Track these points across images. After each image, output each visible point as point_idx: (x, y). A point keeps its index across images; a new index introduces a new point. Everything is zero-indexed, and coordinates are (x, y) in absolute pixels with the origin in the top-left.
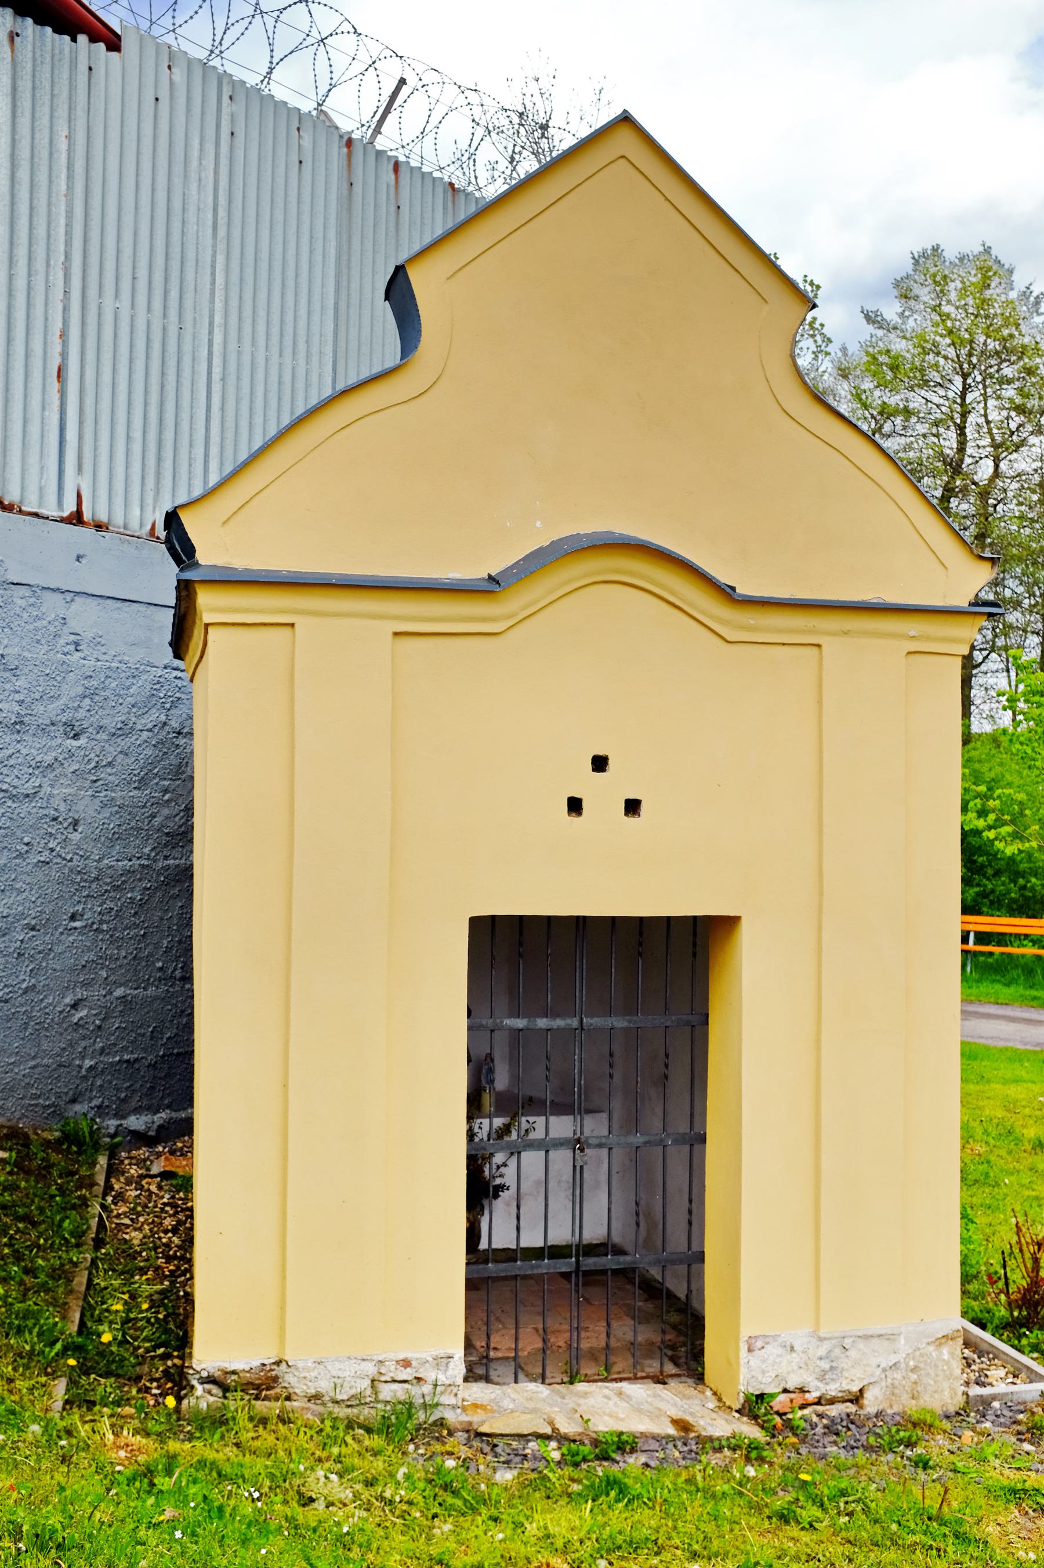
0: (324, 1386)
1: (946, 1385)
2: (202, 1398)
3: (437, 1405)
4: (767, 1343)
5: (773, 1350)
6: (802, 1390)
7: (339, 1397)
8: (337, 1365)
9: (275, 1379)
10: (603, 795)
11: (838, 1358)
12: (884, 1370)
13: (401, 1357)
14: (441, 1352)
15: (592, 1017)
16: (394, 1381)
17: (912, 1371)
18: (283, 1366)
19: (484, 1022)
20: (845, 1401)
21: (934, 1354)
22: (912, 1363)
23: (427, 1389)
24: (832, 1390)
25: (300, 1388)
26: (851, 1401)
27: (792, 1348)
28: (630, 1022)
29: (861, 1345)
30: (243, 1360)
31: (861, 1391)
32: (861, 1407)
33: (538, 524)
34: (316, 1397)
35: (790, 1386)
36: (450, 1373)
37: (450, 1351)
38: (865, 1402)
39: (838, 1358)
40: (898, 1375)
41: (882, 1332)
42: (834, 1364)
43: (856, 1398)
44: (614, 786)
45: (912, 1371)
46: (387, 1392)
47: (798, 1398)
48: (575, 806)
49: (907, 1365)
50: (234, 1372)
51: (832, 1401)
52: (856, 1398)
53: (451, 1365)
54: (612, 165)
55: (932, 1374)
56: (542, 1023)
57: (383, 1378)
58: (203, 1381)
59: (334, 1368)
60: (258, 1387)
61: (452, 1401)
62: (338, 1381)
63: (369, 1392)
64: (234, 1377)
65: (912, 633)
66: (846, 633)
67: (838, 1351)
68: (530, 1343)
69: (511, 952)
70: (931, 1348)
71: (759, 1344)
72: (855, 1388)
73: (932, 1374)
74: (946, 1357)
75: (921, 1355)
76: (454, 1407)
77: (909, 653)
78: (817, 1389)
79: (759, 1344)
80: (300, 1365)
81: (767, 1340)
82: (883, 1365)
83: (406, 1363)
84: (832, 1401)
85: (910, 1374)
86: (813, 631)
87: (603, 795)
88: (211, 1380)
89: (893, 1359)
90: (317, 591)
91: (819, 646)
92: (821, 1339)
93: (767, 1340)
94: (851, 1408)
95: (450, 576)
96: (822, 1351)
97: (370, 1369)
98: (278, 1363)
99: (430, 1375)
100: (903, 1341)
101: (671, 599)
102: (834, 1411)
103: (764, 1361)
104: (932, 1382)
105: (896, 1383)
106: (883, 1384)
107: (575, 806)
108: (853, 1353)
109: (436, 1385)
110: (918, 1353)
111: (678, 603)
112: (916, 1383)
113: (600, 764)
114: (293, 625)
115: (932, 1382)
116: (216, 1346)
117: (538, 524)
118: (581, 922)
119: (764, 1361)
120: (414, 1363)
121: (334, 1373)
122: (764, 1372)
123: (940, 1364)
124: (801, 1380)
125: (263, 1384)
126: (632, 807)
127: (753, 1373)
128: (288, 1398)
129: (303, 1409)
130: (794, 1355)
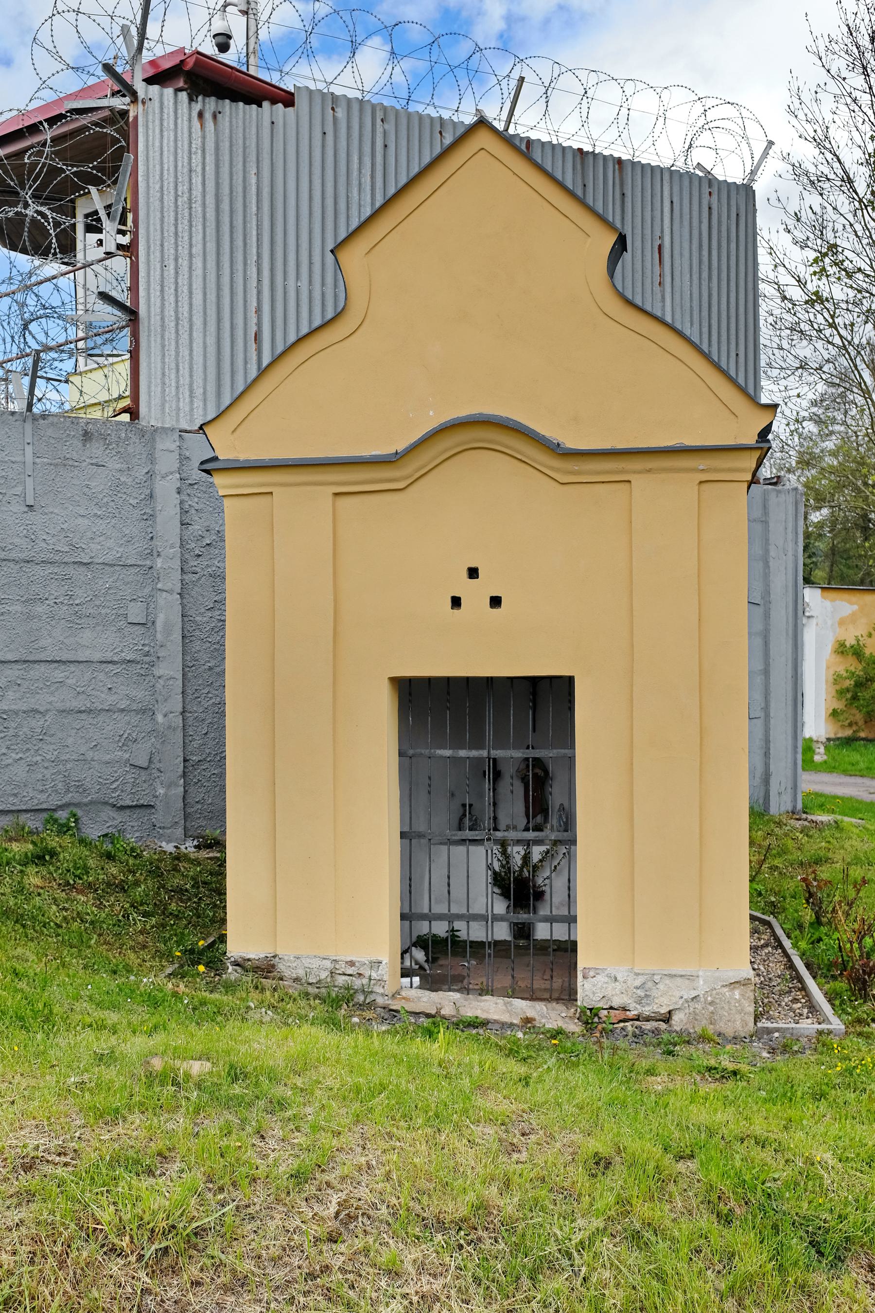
0: (301, 973)
1: (738, 1017)
2: (232, 973)
3: (372, 992)
4: (598, 974)
5: (601, 979)
6: (625, 1009)
7: (311, 981)
8: (308, 960)
9: (273, 966)
10: (475, 595)
11: (650, 989)
12: (687, 1001)
13: (349, 959)
14: (374, 959)
15: (497, 749)
16: (345, 974)
17: (710, 1004)
18: (277, 959)
19: (423, 751)
20: (657, 1020)
21: (727, 994)
22: (709, 998)
23: (365, 981)
24: (647, 1011)
25: (287, 973)
26: (664, 1021)
27: (616, 979)
28: (523, 753)
29: (667, 981)
30: (255, 952)
31: (670, 1012)
32: (670, 1026)
33: (431, 413)
34: (297, 980)
35: (615, 1004)
36: (380, 972)
37: (380, 959)
38: (673, 1022)
39: (650, 989)
40: (699, 1006)
41: (683, 973)
42: (648, 993)
43: (667, 1018)
44: (483, 588)
45: (710, 1004)
46: (341, 980)
47: (620, 1015)
48: (456, 602)
49: (706, 999)
50: (249, 960)
51: (648, 1019)
52: (667, 1018)
53: (381, 968)
54: (476, 156)
55: (727, 1008)
56: (463, 753)
57: (338, 972)
58: (236, 964)
59: (306, 962)
60: (263, 970)
61: (381, 991)
62: (308, 970)
63: (329, 980)
64: (250, 963)
65: (701, 467)
66: (649, 471)
67: (650, 984)
68: (507, 981)
69: (426, 703)
70: (725, 990)
71: (592, 973)
72: (664, 1010)
73: (727, 1008)
74: (737, 997)
75: (717, 994)
76: (382, 995)
77: (701, 482)
78: (636, 1009)
79: (592, 973)
80: (286, 958)
81: (597, 971)
82: (685, 997)
83: (352, 964)
84: (648, 1019)
85: (708, 1006)
86: (623, 471)
87: (475, 595)
88: (236, 964)
89: (693, 994)
90: (310, 469)
91: (629, 481)
92: (637, 974)
93: (597, 971)
94: (663, 1026)
95: (374, 453)
96: (638, 983)
97: (328, 964)
98: (274, 957)
99: (367, 973)
100: (701, 982)
101: (519, 457)
102: (648, 1026)
103: (594, 986)
104: (726, 1014)
105: (697, 1011)
106: (687, 1011)
107: (456, 602)
108: (661, 986)
109: (370, 979)
110: (714, 992)
111: (524, 459)
112: (712, 1013)
113: (473, 573)
114: (271, 493)
115: (726, 1014)
116: (242, 942)
117: (431, 413)
118: (468, 681)
119: (594, 986)
120: (357, 964)
121: (306, 965)
122: (594, 993)
123: (733, 1002)
124: (622, 1001)
125: (265, 969)
126: (496, 602)
127: (587, 993)
128: (282, 979)
129: (290, 986)
130: (617, 984)
